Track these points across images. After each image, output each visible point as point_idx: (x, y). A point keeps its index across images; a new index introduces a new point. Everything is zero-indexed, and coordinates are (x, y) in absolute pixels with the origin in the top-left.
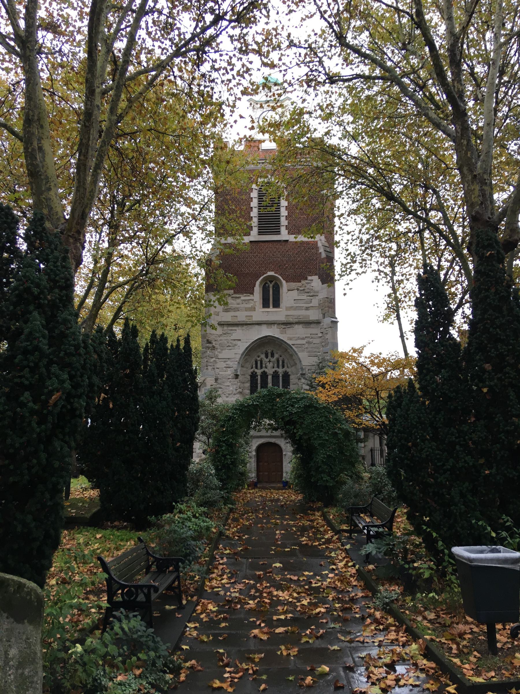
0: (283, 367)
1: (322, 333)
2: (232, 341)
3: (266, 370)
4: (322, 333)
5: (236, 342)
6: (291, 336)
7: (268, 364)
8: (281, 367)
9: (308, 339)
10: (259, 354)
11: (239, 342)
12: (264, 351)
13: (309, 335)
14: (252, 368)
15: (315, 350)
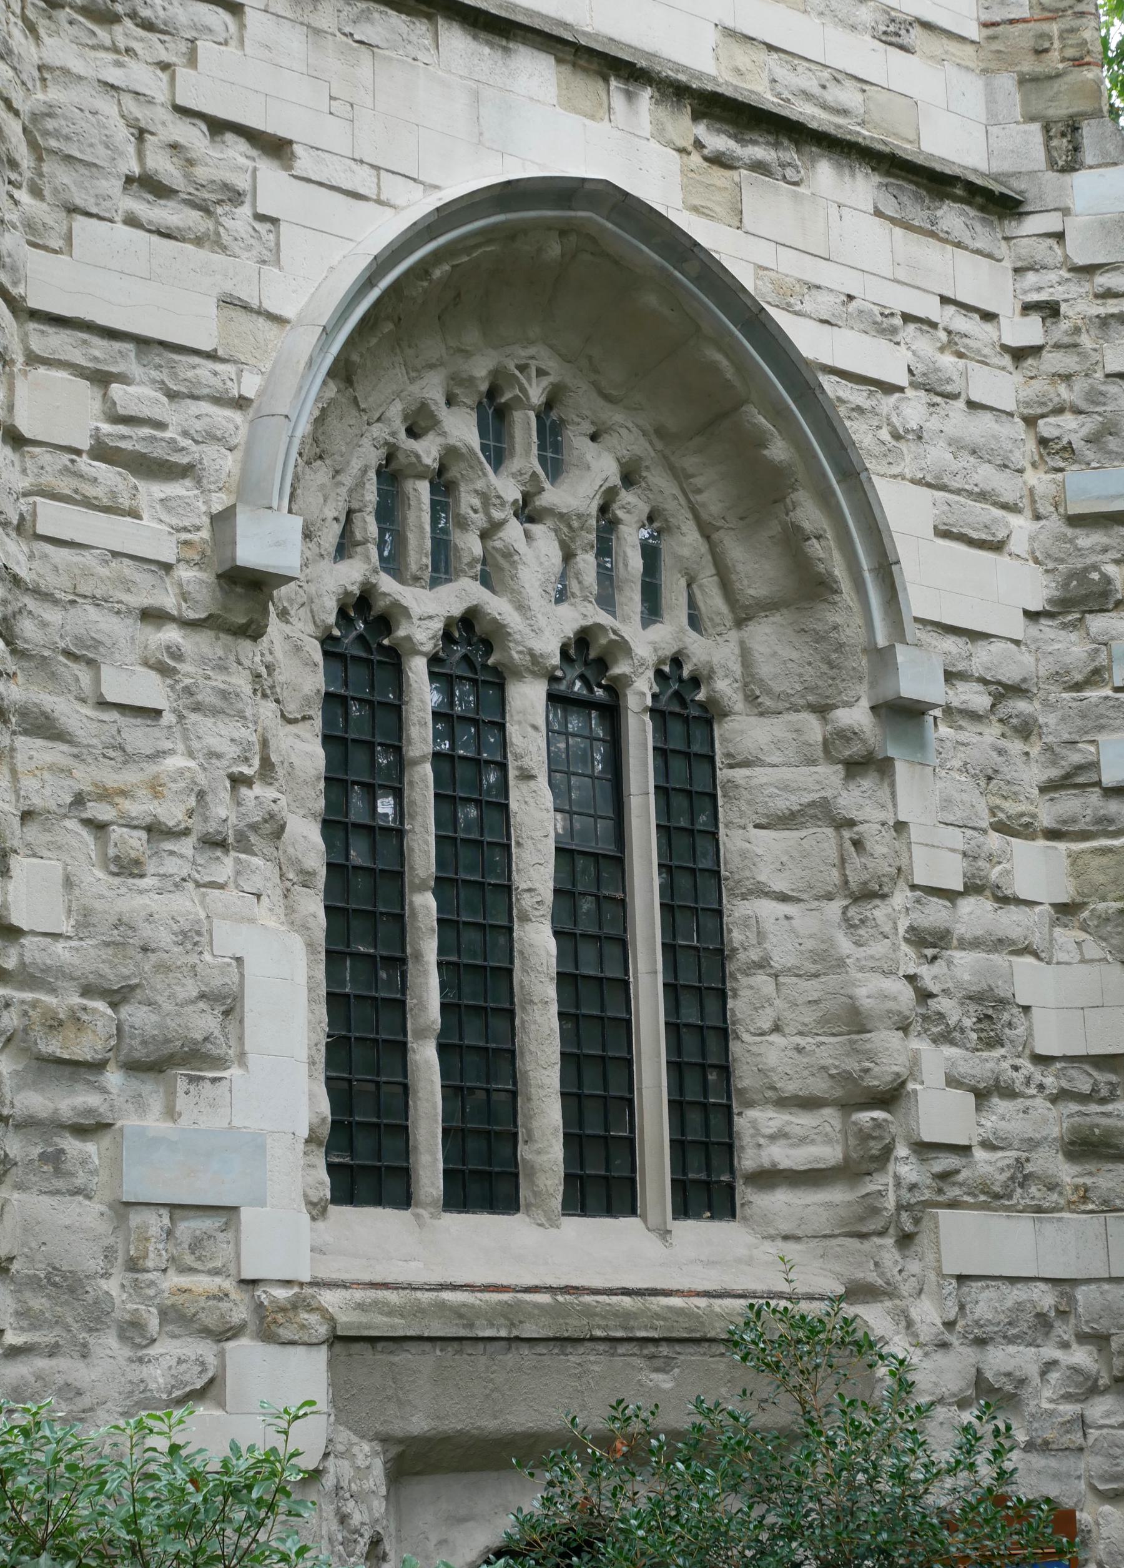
0: (652, 609)
1: (1050, 310)
2: (194, 136)
3: (498, 606)
4: (1050, 310)
5: (237, 150)
6: (792, 266)
7: (513, 532)
8: (632, 599)
9: (924, 345)
10: (432, 389)
11: (269, 172)
12: (481, 369)
13: (929, 308)
14: (345, 548)
15: (986, 476)
